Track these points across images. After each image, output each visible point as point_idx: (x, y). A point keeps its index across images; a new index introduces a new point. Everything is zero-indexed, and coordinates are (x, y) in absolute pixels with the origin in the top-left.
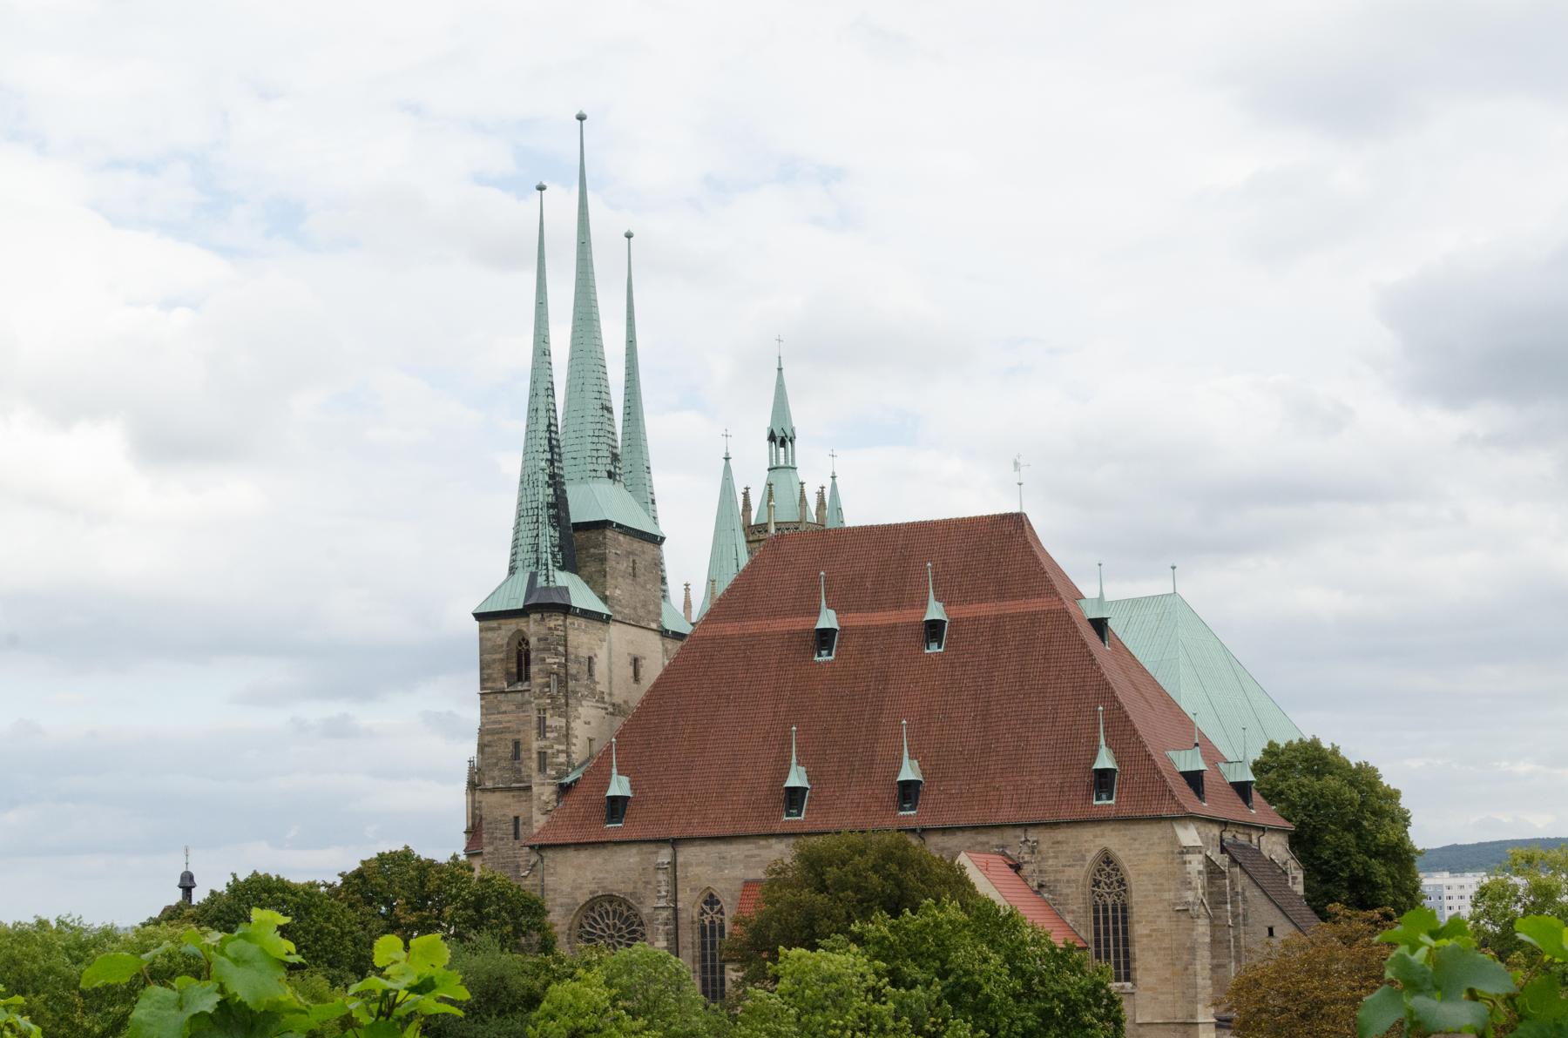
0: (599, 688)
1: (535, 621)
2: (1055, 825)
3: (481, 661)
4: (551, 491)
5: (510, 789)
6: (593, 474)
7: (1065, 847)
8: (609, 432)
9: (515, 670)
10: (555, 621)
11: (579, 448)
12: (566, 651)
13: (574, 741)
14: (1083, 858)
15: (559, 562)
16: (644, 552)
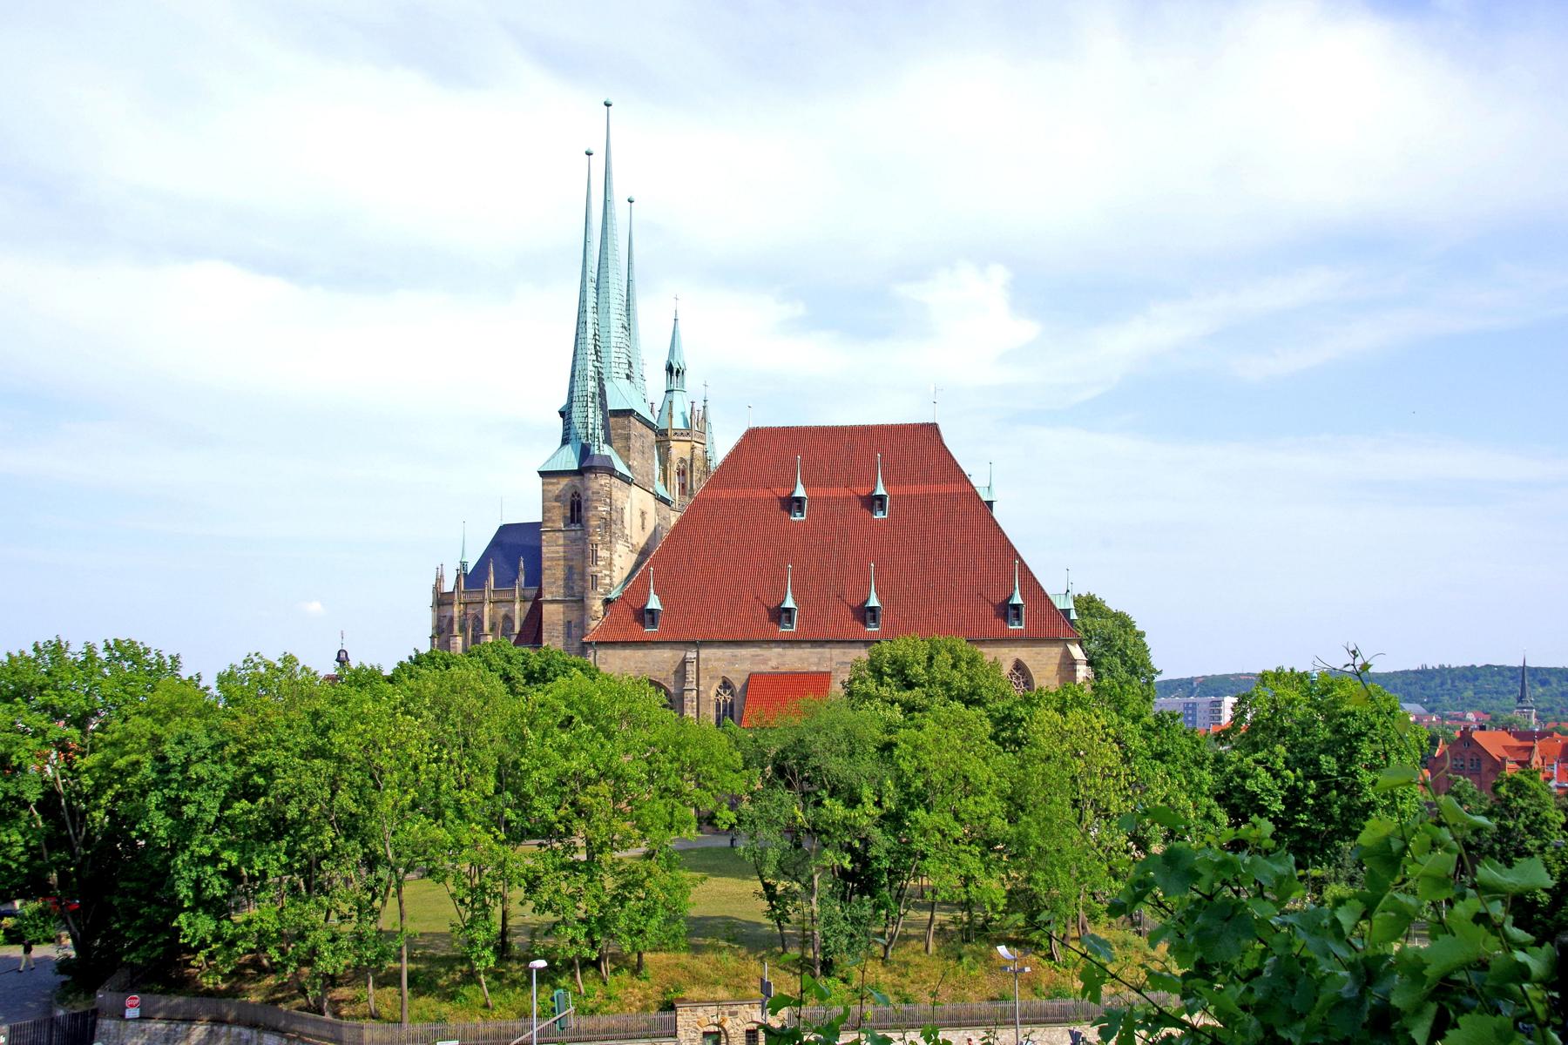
6: (616, 375)
9: (569, 515)
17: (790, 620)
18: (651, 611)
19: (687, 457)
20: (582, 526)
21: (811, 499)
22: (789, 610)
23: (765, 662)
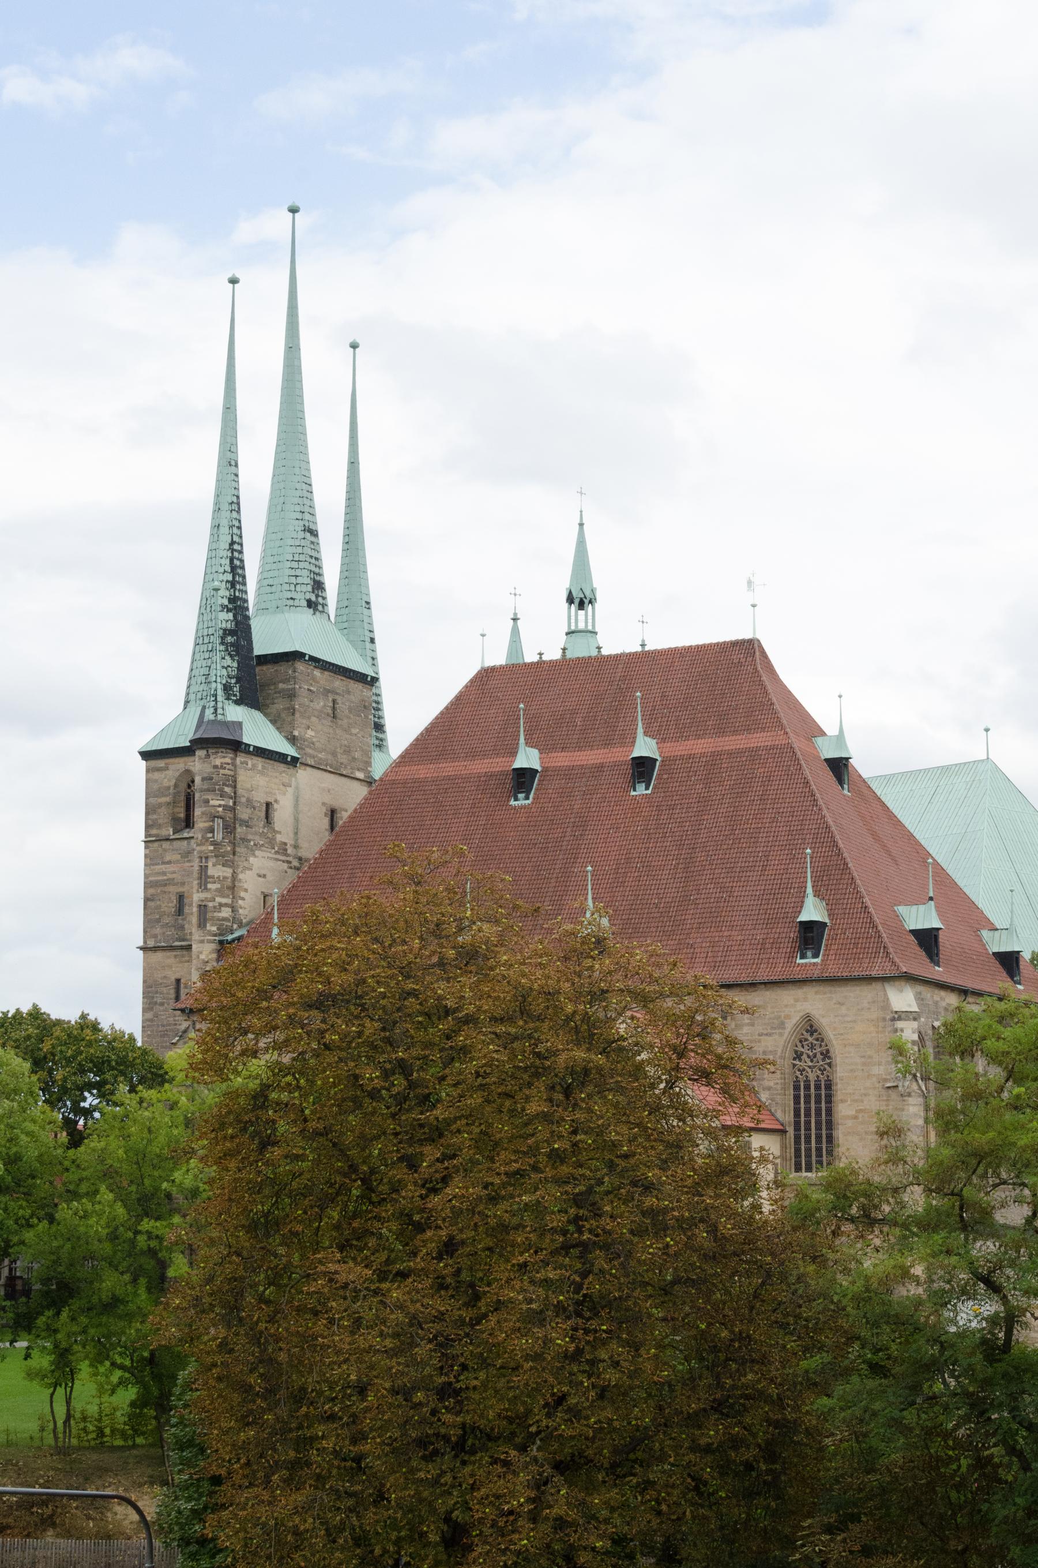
0: (279, 838)
1: (200, 758)
2: (753, 985)
3: (147, 805)
4: (230, 616)
5: (172, 948)
6: (291, 602)
8: (311, 557)
9: (182, 815)
10: (221, 758)
11: (276, 573)
12: (235, 793)
13: (242, 894)
14: (782, 1026)
15: (235, 695)
16: (349, 692)
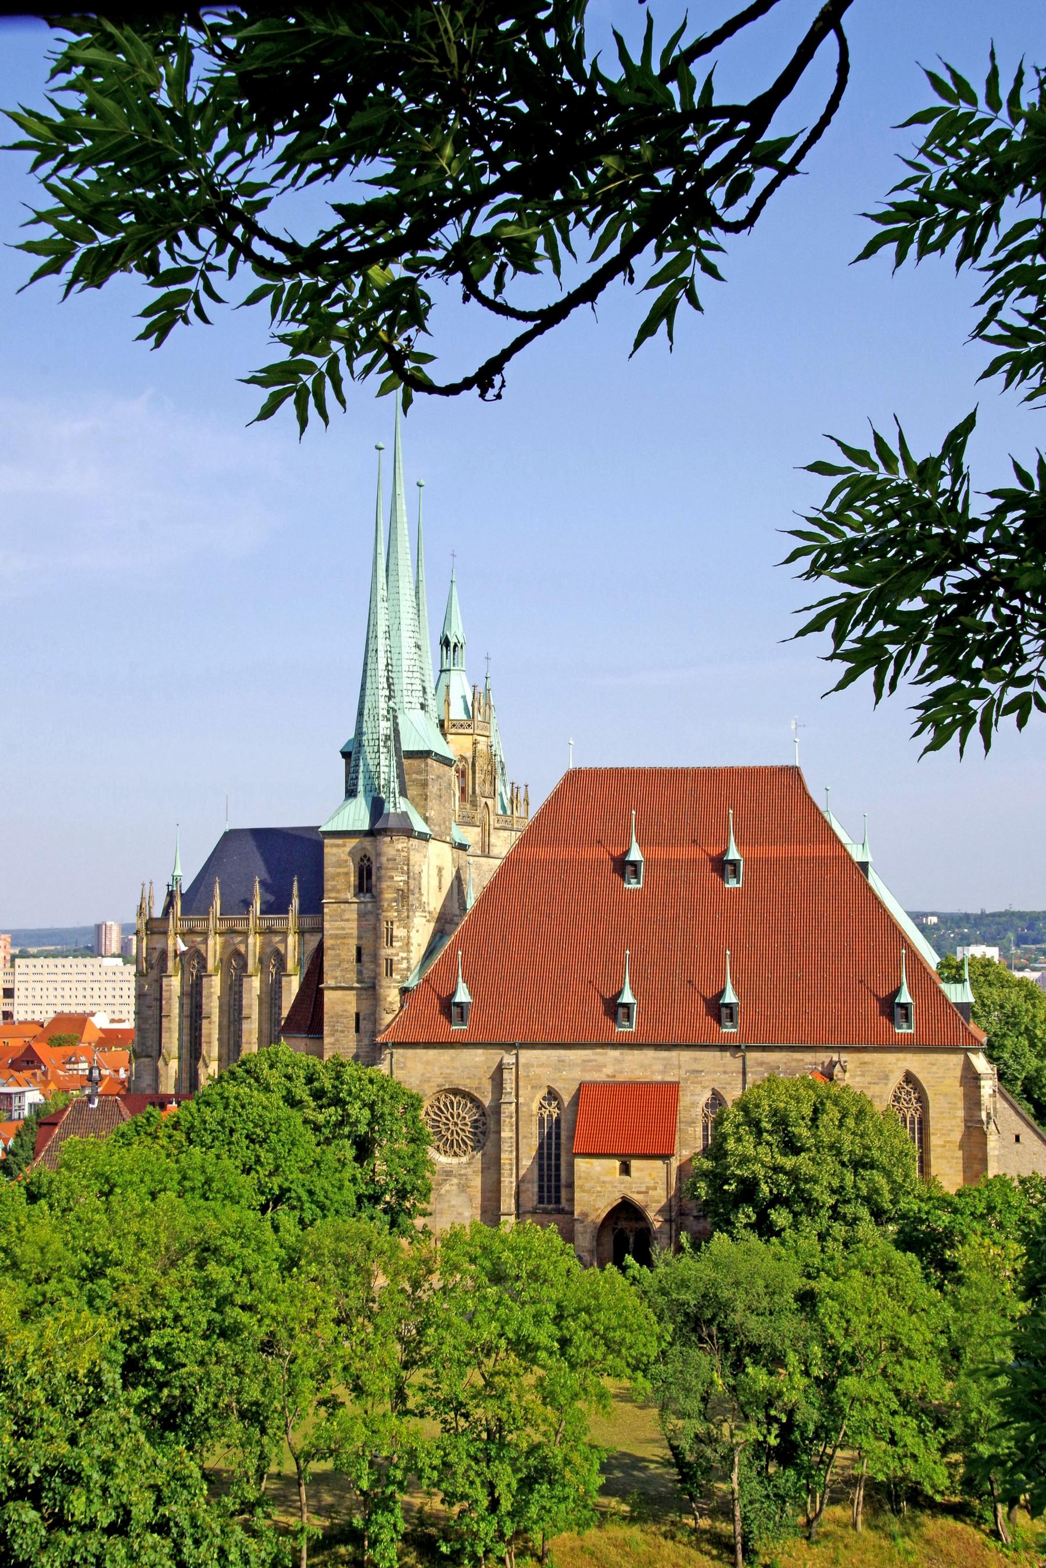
4: (389, 724)
7: (871, 1067)
14: (886, 1077)
17: (628, 1017)
18: (459, 1005)
19: (469, 754)
20: (373, 897)
21: (647, 860)
22: (627, 1006)
23: (599, 1068)
